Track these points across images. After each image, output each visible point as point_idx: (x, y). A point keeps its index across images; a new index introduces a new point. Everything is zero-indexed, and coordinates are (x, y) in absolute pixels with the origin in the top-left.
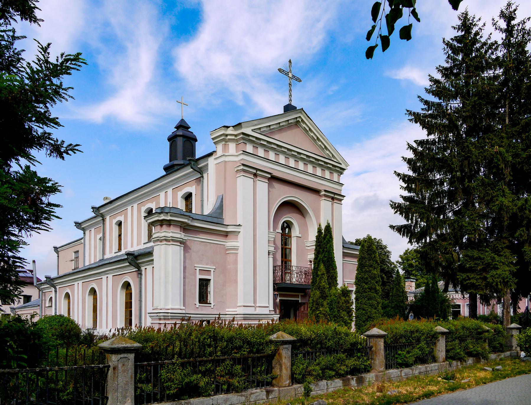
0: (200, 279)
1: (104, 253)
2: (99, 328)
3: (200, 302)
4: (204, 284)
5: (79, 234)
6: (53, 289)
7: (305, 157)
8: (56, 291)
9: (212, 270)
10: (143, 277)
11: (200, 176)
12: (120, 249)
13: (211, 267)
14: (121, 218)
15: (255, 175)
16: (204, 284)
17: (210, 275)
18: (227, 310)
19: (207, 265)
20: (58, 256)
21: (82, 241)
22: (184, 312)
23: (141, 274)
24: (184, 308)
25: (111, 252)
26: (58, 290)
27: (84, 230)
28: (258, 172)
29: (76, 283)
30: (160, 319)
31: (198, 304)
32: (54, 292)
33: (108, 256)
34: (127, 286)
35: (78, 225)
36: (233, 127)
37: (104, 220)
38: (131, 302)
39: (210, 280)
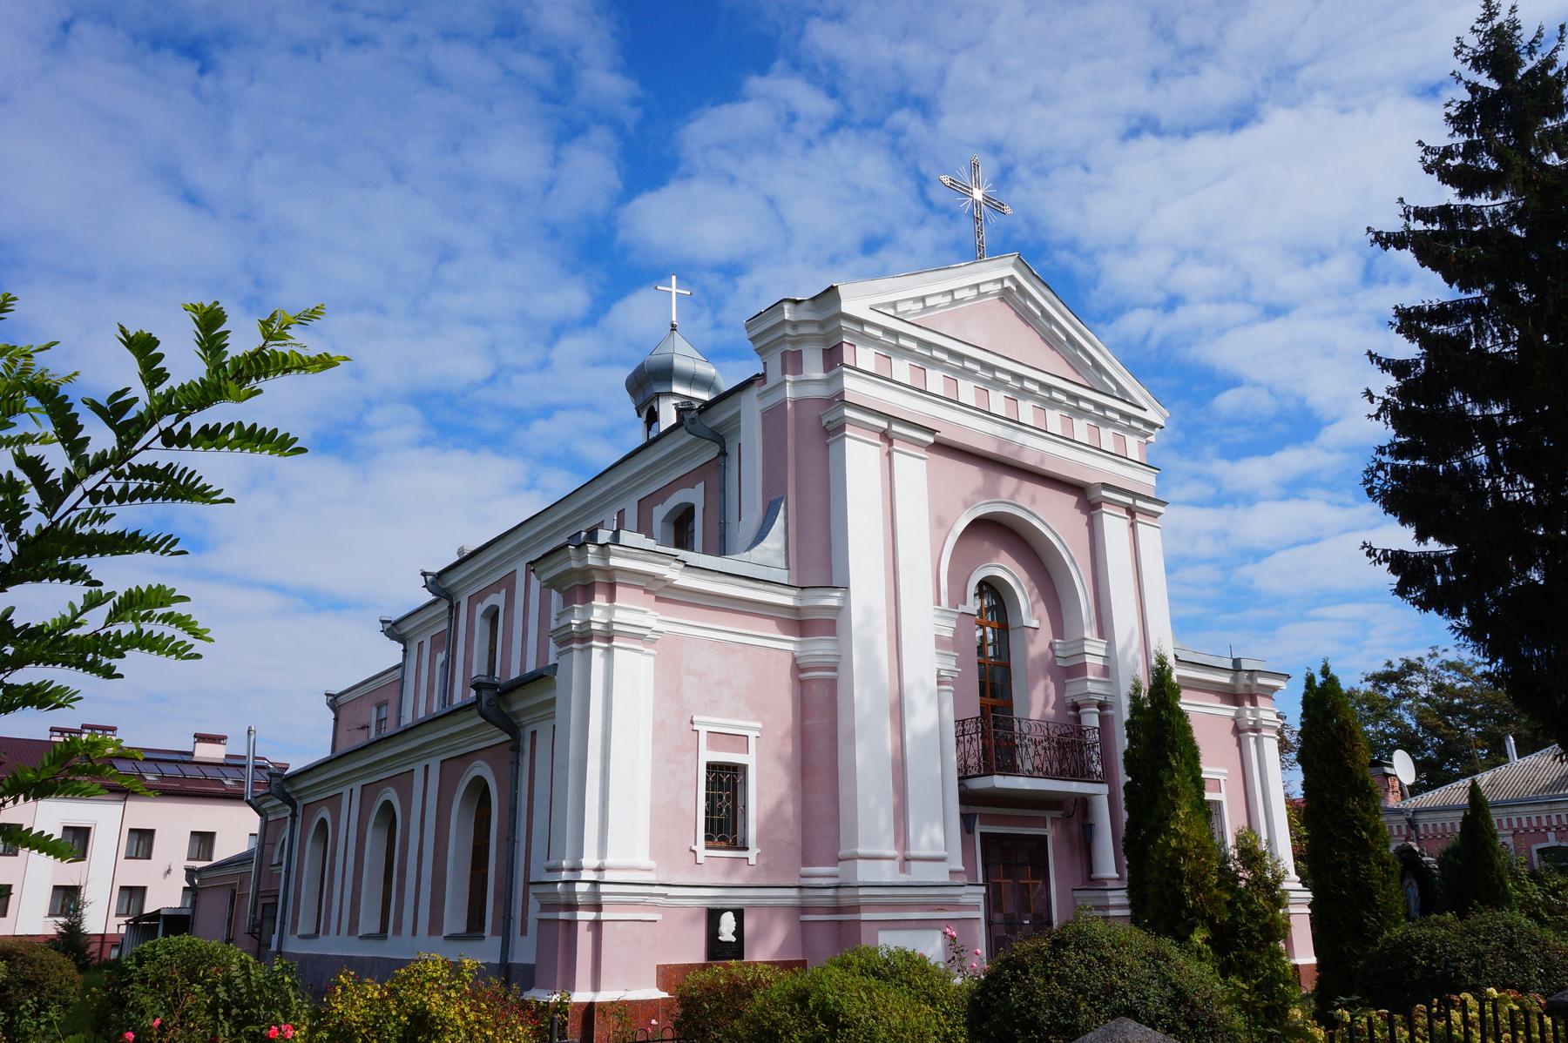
0: (711, 767)
2: (394, 933)
4: (725, 782)
5: (393, 653)
8: (294, 815)
9: (752, 735)
13: (749, 726)
14: (498, 599)
15: (886, 436)
16: (725, 782)
19: (736, 715)
20: (336, 719)
21: (398, 671)
22: (651, 878)
23: (516, 748)
24: (653, 864)
26: (300, 811)
27: (402, 639)
28: (895, 428)
29: (345, 791)
36: (813, 299)
37: (454, 608)
39: (744, 767)
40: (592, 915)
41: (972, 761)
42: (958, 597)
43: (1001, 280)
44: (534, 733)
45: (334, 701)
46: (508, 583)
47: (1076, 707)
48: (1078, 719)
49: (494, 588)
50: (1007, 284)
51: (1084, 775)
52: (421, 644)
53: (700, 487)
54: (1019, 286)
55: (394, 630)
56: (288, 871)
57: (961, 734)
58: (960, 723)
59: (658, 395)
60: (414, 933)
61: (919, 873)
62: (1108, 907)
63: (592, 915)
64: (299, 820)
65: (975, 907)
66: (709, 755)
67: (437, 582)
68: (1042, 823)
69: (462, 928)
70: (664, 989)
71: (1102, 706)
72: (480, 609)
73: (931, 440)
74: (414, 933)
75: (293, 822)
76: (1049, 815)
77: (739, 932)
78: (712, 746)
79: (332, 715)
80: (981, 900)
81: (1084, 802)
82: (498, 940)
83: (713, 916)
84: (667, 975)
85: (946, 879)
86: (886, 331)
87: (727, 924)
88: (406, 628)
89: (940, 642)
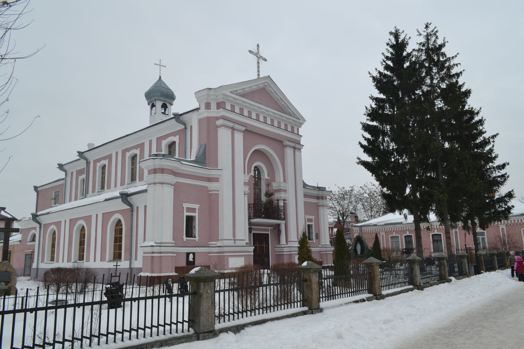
0: (187, 216)
3: (187, 236)
4: (190, 220)
5: (62, 175)
6: (38, 226)
7: (272, 114)
8: (40, 227)
10: (135, 214)
11: (182, 127)
13: (197, 206)
14: (106, 162)
15: (233, 129)
16: (190, 220)
17: (195, 212)
18: (210, 243)
20: (38, 195)
21: (64, 180)
22: (173, 245)
23: (132, 211)
24: (174, 242)
26: (42, 226)
27: (65, 171)
28: (237, 126)
30: (153, 253)
31: (185, 238)
32: (38, 229)
34: (119, 223)
35: (61, 167)
37: (88, 163)
38: (121, 238)
41: (252, 215)
42: (249, 172)
43: (264, 83)
44: (138, 207)
45: (36, 188)
46: (109, 157)
47: (278, 200)
48: (278, 203)
49: (104, 158)
50: (266, 84)
51: (279, 219)
52: (72, 173)
53: (178, 137)
54: (269, 85)
55: (61, 167)
56: (39, 244)
57: (249, 207)
58: (249, 205)
59: (156, 100)
60: (95, 261)
61: (238, 243)
62: (283, 252)
64: (42, 229)
65: (251, 252)
66: (186, 214)
67: (81, 154)
68: (268, 230)
69: (112, 259)
70: (176, 272)
71: (284, 200)
72: (99, 165)
73: (244, 129)
74: (95, 261)
75: (40, 229)
76: (269, 228)
77: (194, 258)
78: (187, 211)
79: (36, 194)
80: (252, 250)
81: (279, 225)
82: (128, 262)
83: (188, 254)
84: (177, 269)
85: (245, 245)
86: (234, 98)
87: (191, 256)
88: (66, 167)
89: (245, 184)
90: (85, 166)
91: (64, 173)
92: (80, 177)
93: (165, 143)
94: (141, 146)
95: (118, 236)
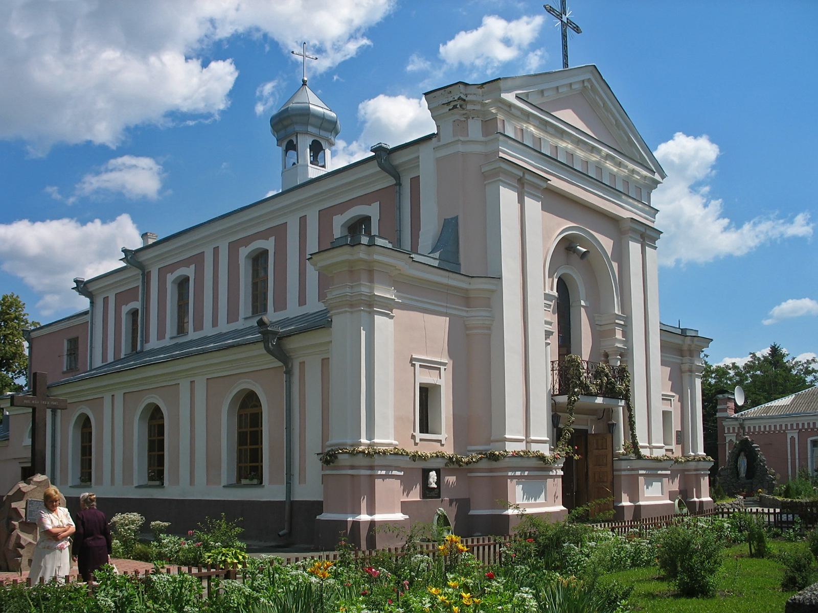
1: (146, 340)
5: (83, 303)
11: (391, 181)
12: (181, 329)
14: (190, 271)
16: (427, 393)
21: (88, 318)
25: (161, 335)
31: (419, 436)
33: (154, 343)
35: (82, 287)
37: (146, 277)
40: (368, 472)
49: (186, 263)
52: (106, 300)
53: (376, 205)
63: (368, 472)
72: (170, 278)
77: (438, 482)
83: (426, 473)
88: (92, 288)
90: (140, 283)
91: (88, 300)
92: (123, 307)
93: (339, 222)
94: (279, 232)
95: (249, 430)
